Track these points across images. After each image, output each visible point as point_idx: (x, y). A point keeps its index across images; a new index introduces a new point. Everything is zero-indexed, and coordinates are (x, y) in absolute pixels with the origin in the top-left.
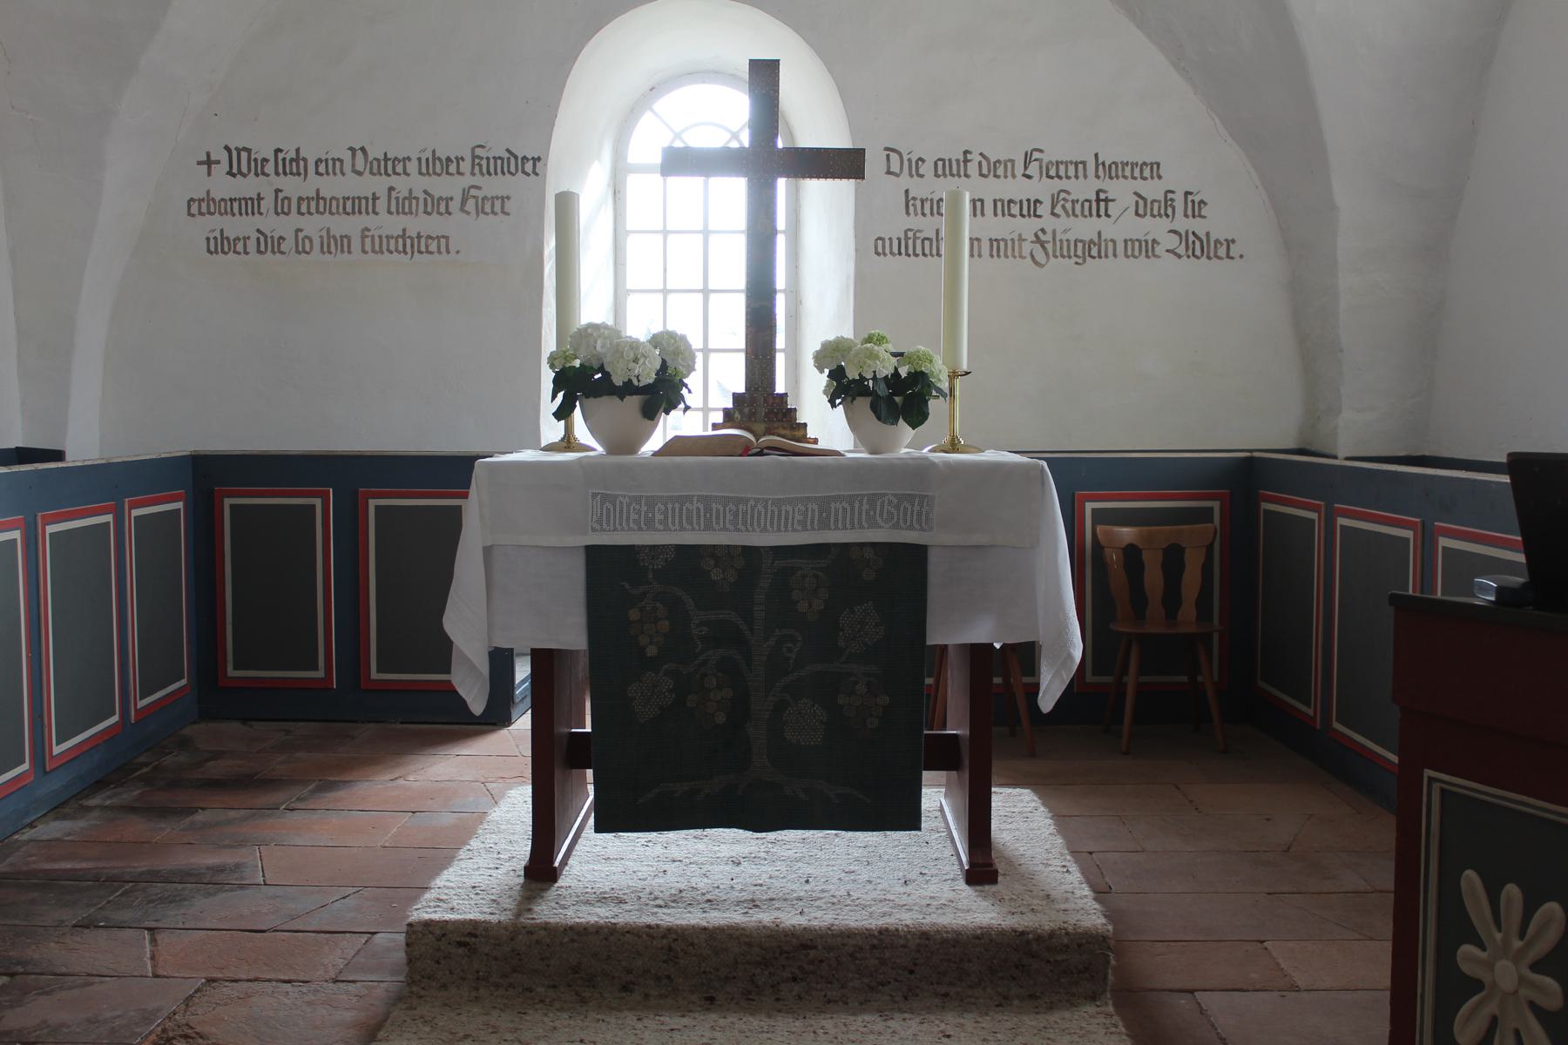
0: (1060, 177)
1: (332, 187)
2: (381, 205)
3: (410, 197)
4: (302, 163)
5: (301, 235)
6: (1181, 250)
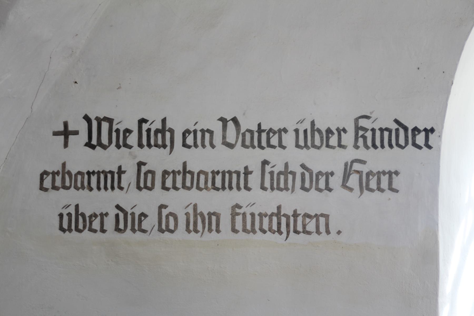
2: (254, 180)
3: (286, 172)
4: (168, 135)
5: (165, 212)
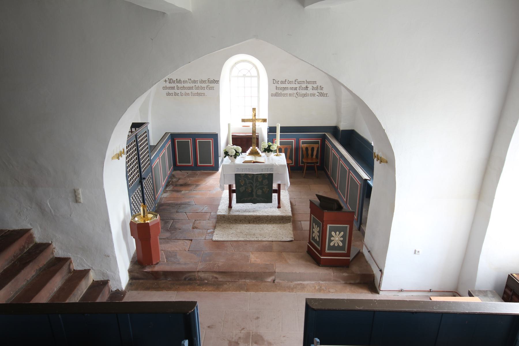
0: (300, 84)
1: (186, 85)
2: (194, 88)
3: (198, 87)
6: (319, 95)
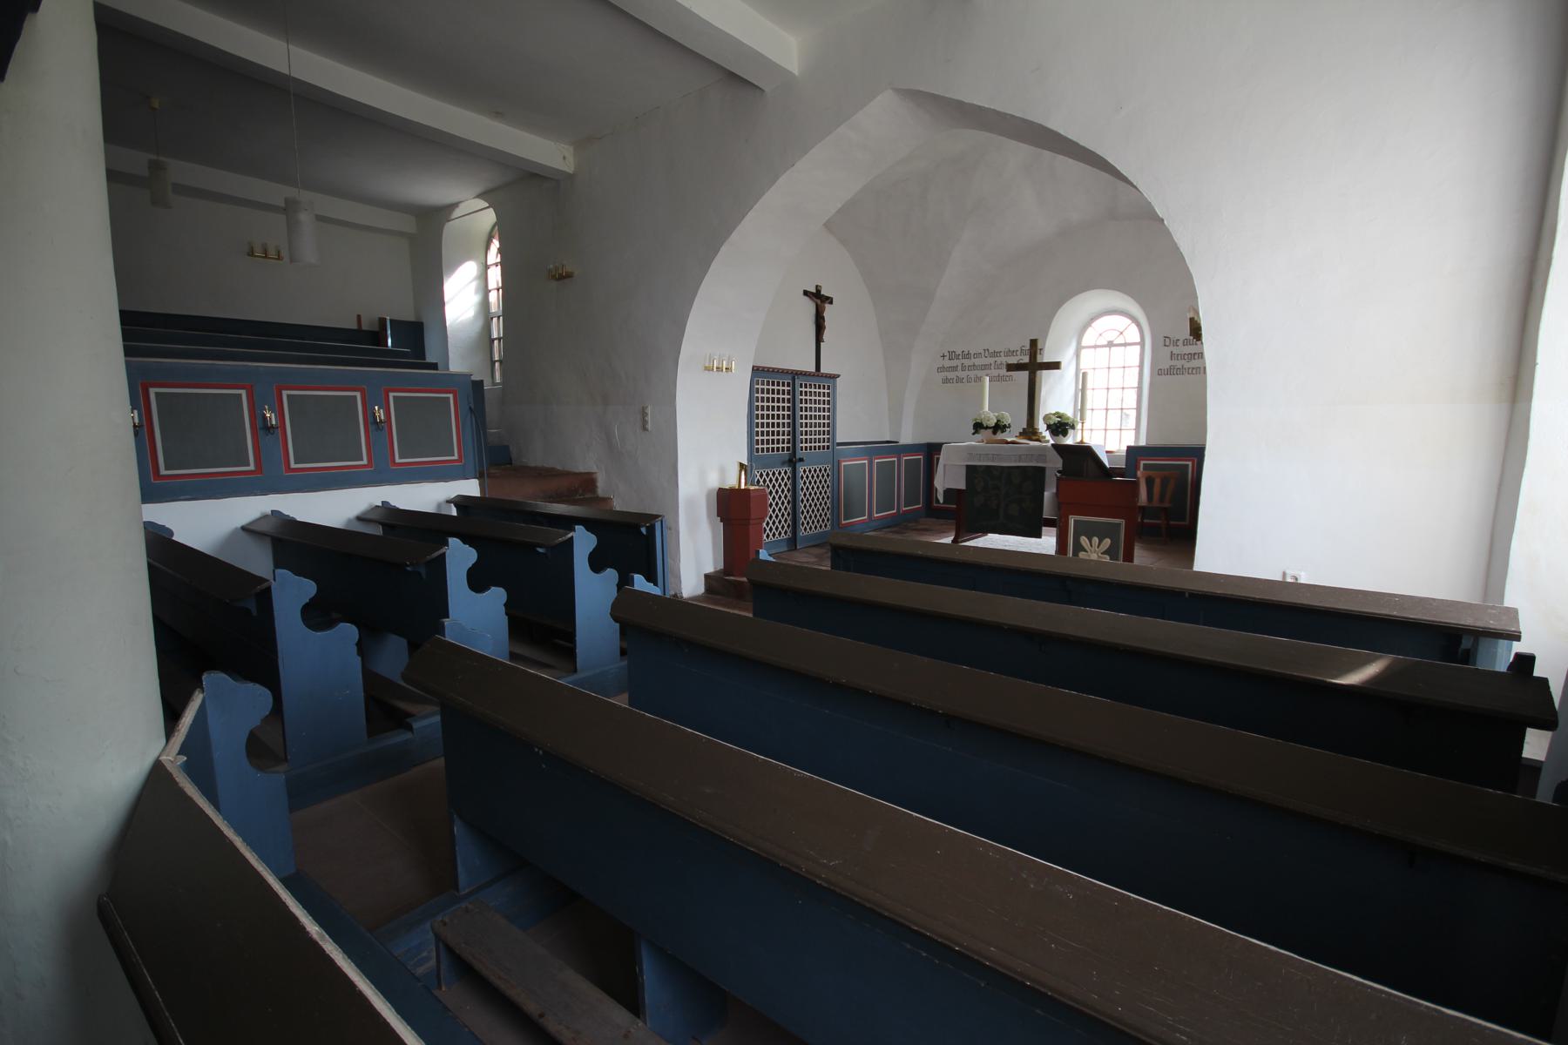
1: (978, 362)
2: (992, 367)
3: (1001, 364)
